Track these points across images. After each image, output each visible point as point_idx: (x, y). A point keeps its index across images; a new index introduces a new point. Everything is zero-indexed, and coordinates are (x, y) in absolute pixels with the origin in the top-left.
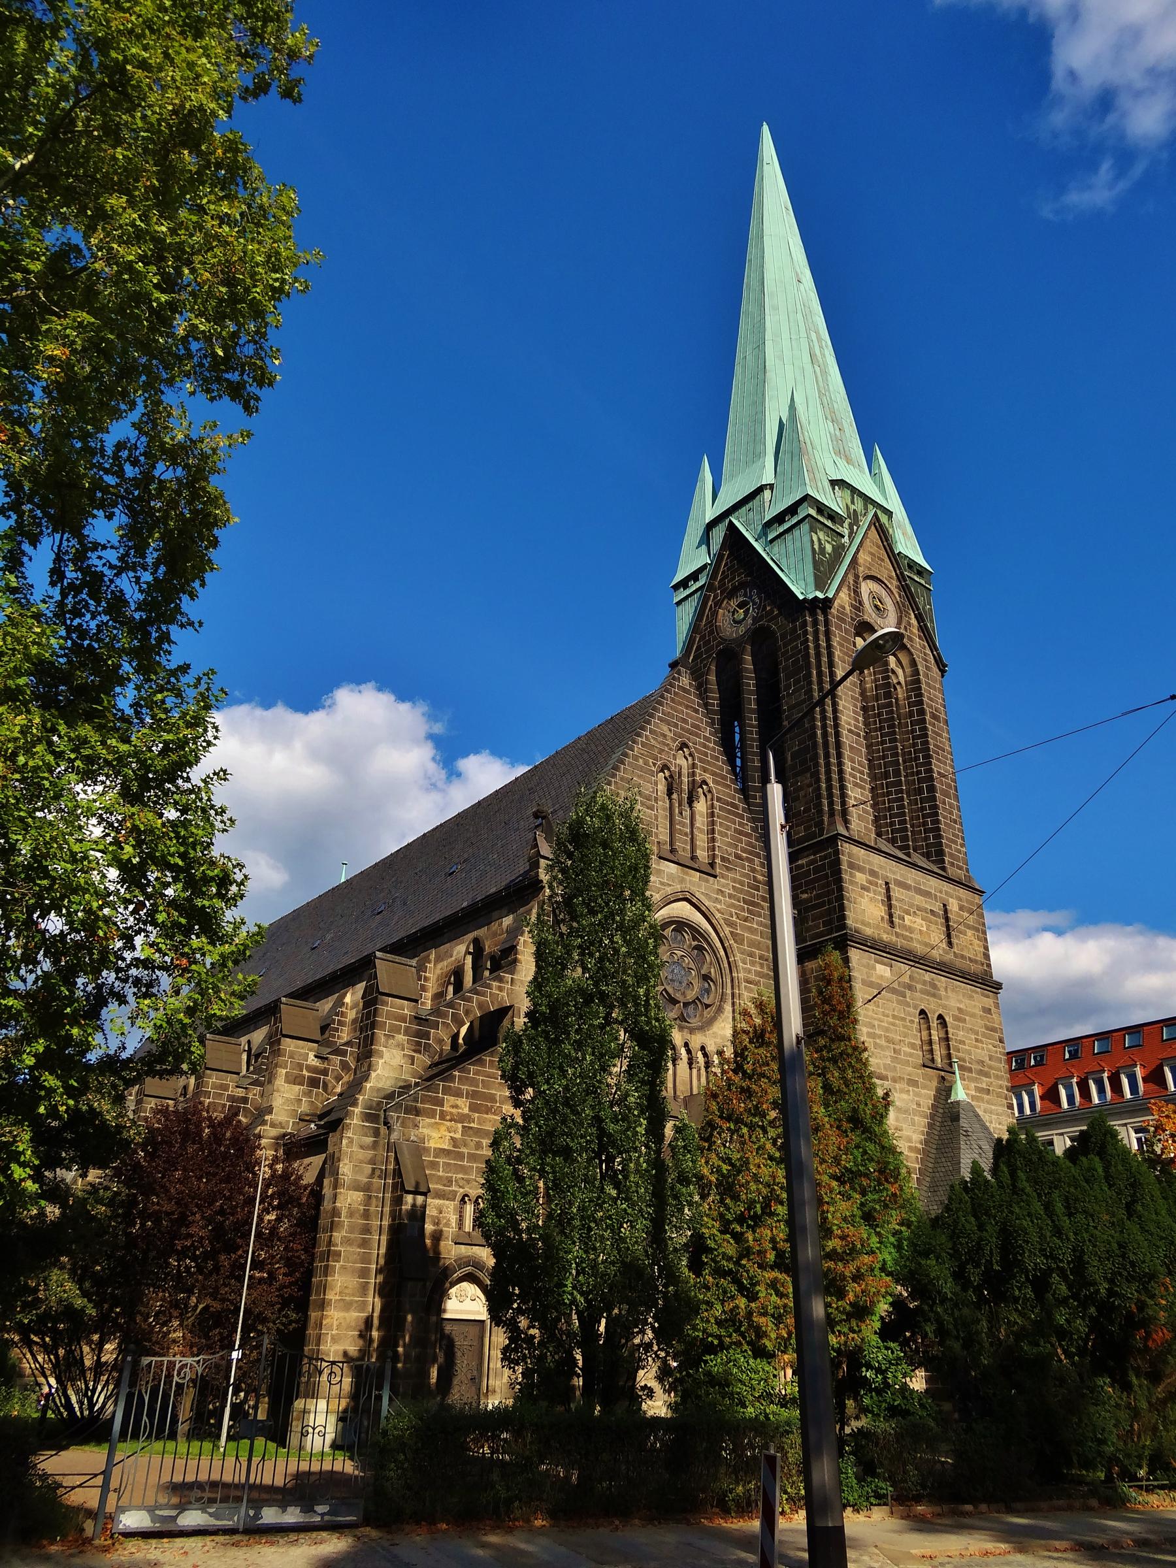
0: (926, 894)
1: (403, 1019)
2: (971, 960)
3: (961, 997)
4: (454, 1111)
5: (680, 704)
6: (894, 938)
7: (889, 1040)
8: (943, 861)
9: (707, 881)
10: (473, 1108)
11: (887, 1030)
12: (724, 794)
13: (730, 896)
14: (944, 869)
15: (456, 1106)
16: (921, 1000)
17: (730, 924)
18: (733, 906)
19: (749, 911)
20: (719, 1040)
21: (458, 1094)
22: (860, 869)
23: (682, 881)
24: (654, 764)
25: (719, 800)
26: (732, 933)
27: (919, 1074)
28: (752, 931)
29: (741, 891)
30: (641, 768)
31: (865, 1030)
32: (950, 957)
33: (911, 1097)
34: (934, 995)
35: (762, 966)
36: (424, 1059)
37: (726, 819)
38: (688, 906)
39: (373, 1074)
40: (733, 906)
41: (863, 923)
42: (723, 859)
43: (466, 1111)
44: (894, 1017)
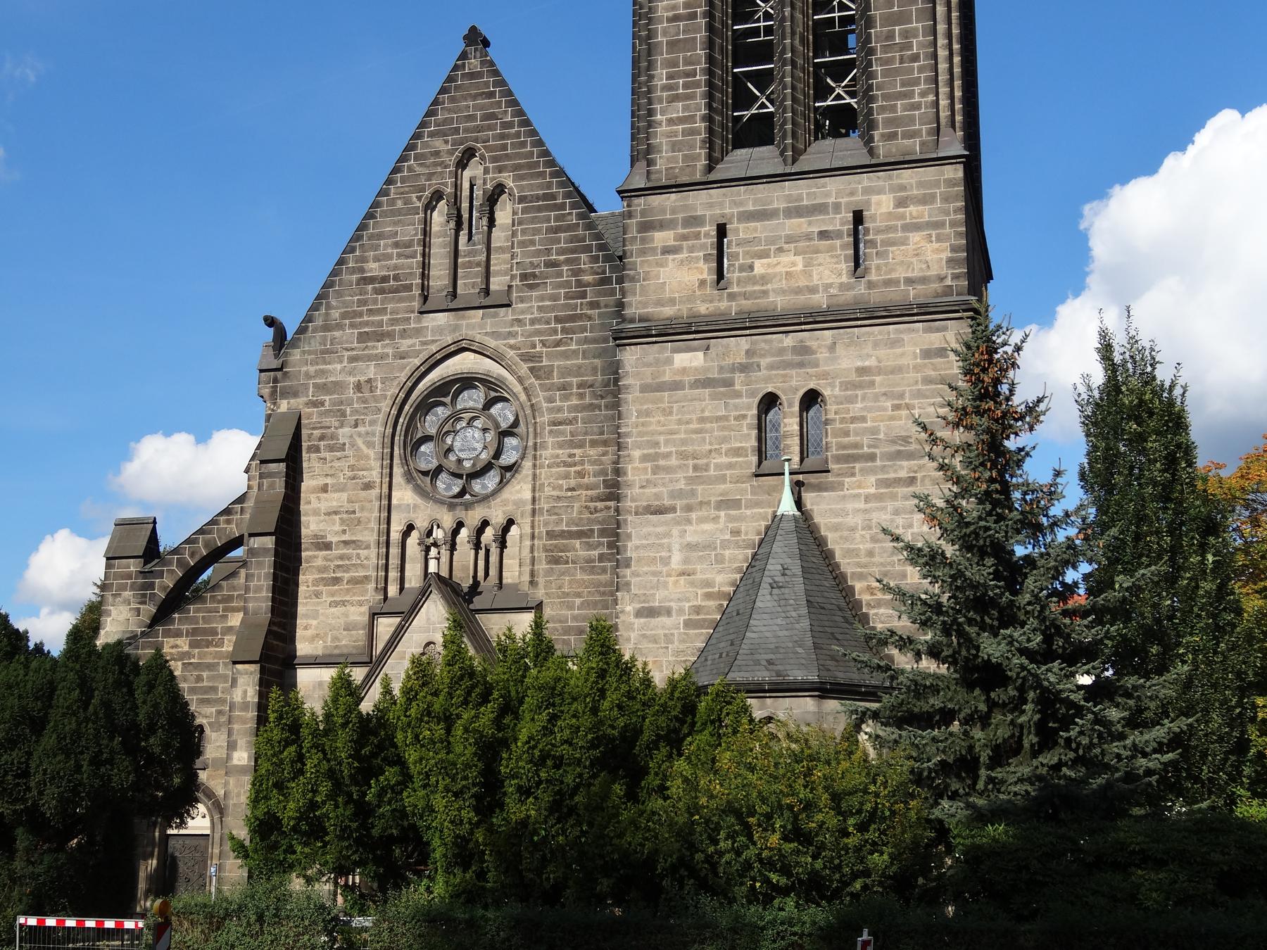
0: (820, 209)
1: (129, 576)
2: (909, 281)
3: (868, 349)
4: (173, 651)
5: (465, 98)
6: (723, 305)
7: (683, 455)
8: (871, 139)
9: (496, 315)
10: (193, 645)
11: (684, 442)
12: (531, 187)
13: (533, 322)
14: (871, 152)
15: (176, 646)
16: (768, 380)
17: (526, 358)
18: (538, 333)
19: (564, 330)
20: (510, 508)
21: (178, 634)
22: (662, 226)
23: (456, 328)
24: (419, 198)
25: (522, 199)
26: (531, 369)
27: (746, 491)
28: (565, 355)
29: (553, 308)
30: (399, 212)
31: (637, 454)
32: (861, 289)
33: (721, 526)
34: (801, 365)
35: (581, 396)
36: (151, 609)
37: (533, 220)
38: (471, 355)
39: (102, 632)
40: (538, 333)
41: (660, 303)
42: (524, 277)
43: (186, 648)
44: (702, 420)
